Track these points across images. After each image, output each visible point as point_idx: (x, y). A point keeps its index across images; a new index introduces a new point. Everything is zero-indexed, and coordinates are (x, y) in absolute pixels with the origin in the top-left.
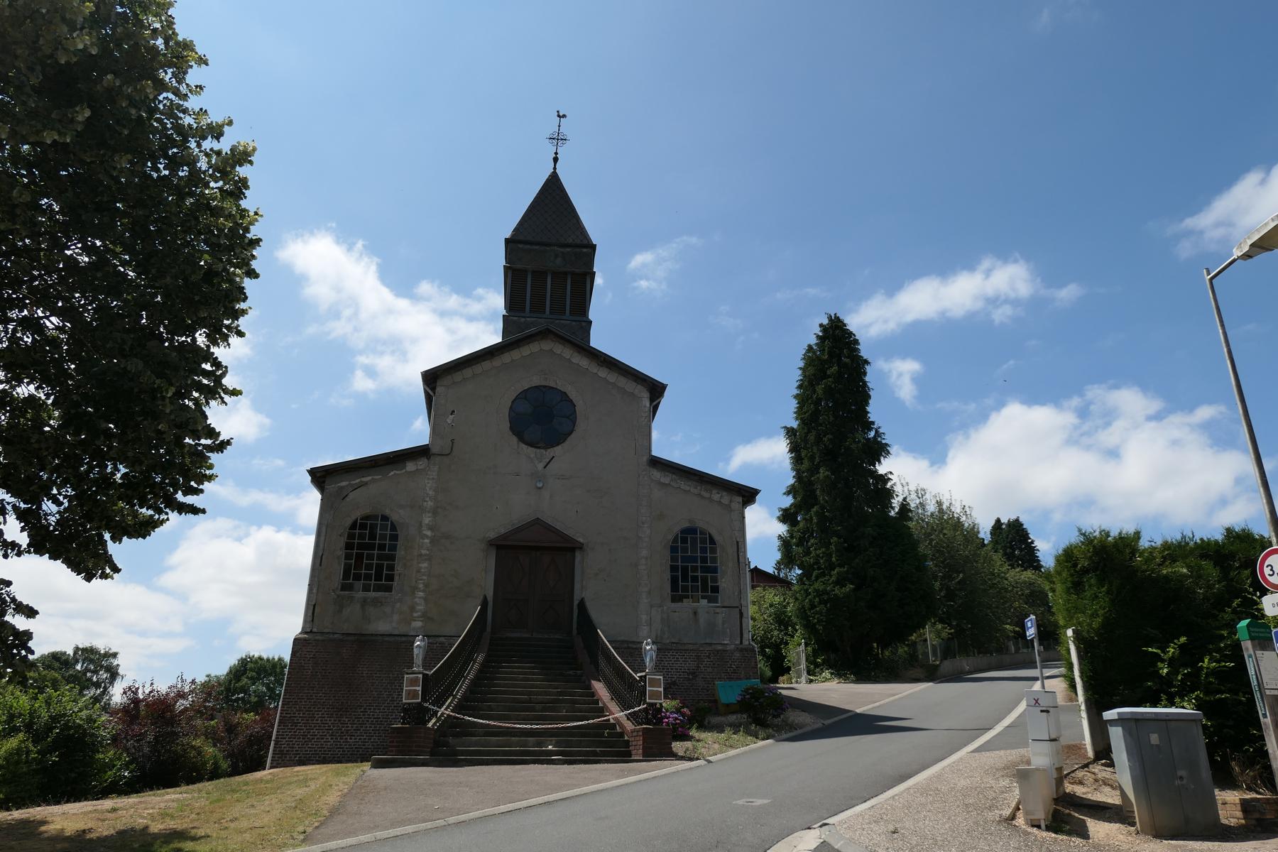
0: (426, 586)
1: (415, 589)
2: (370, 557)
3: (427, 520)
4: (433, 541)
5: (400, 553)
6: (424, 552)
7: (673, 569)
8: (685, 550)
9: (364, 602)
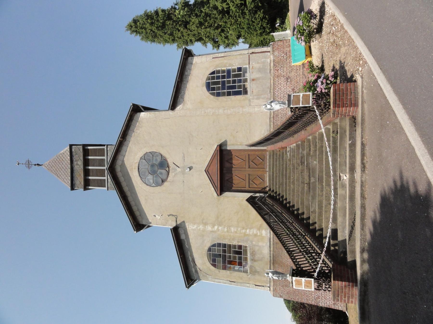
0: (243, 228)
1: (245, 235)
2: (230, 257)
3: (209, 228)
4: (220, 224)
5: (227, 242)
6: (226, 230)
7: (229, 94)
8: (218, 88)
9: (253, 260)
